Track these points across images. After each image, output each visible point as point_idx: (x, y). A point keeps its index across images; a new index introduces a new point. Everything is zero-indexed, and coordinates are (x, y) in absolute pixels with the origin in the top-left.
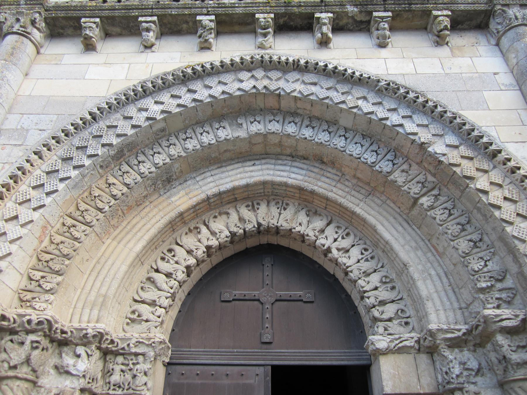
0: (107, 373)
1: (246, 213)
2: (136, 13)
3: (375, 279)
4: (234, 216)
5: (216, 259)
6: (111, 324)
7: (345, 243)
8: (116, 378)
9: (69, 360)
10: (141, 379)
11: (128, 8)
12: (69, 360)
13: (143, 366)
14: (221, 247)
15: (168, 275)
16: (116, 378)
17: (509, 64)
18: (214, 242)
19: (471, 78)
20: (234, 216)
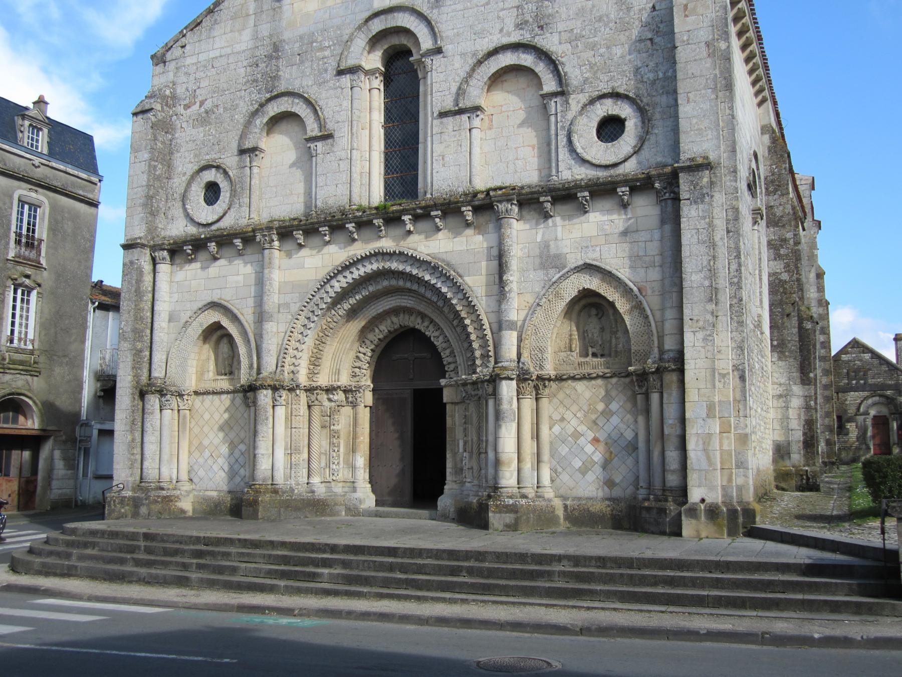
0: (347, 398)
1: (395, 319)
2: (317, 226)
3: (448, 352)
4: (389, 321)
5: (383, 345)
6: (344, 380)
7: (437, 334)
8: (350, 399)
9: (331, 396)
10: (359, 400)
11: (312, 223)
12: (331, 396)
13: (359, 395)
14: (385, 337)
15: (364, 354)
16: (350, 399)
17: (494, 243)
18: (381, 336)
19: (478, 252)
20: (389, 321)
